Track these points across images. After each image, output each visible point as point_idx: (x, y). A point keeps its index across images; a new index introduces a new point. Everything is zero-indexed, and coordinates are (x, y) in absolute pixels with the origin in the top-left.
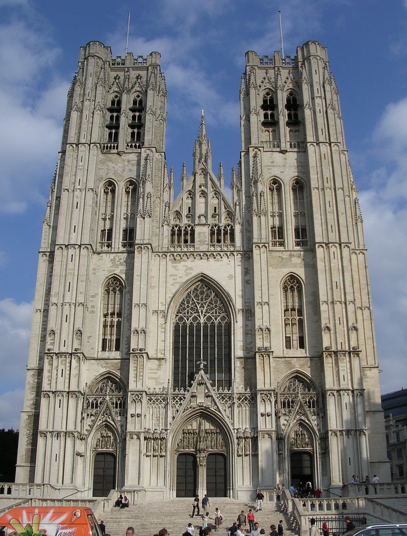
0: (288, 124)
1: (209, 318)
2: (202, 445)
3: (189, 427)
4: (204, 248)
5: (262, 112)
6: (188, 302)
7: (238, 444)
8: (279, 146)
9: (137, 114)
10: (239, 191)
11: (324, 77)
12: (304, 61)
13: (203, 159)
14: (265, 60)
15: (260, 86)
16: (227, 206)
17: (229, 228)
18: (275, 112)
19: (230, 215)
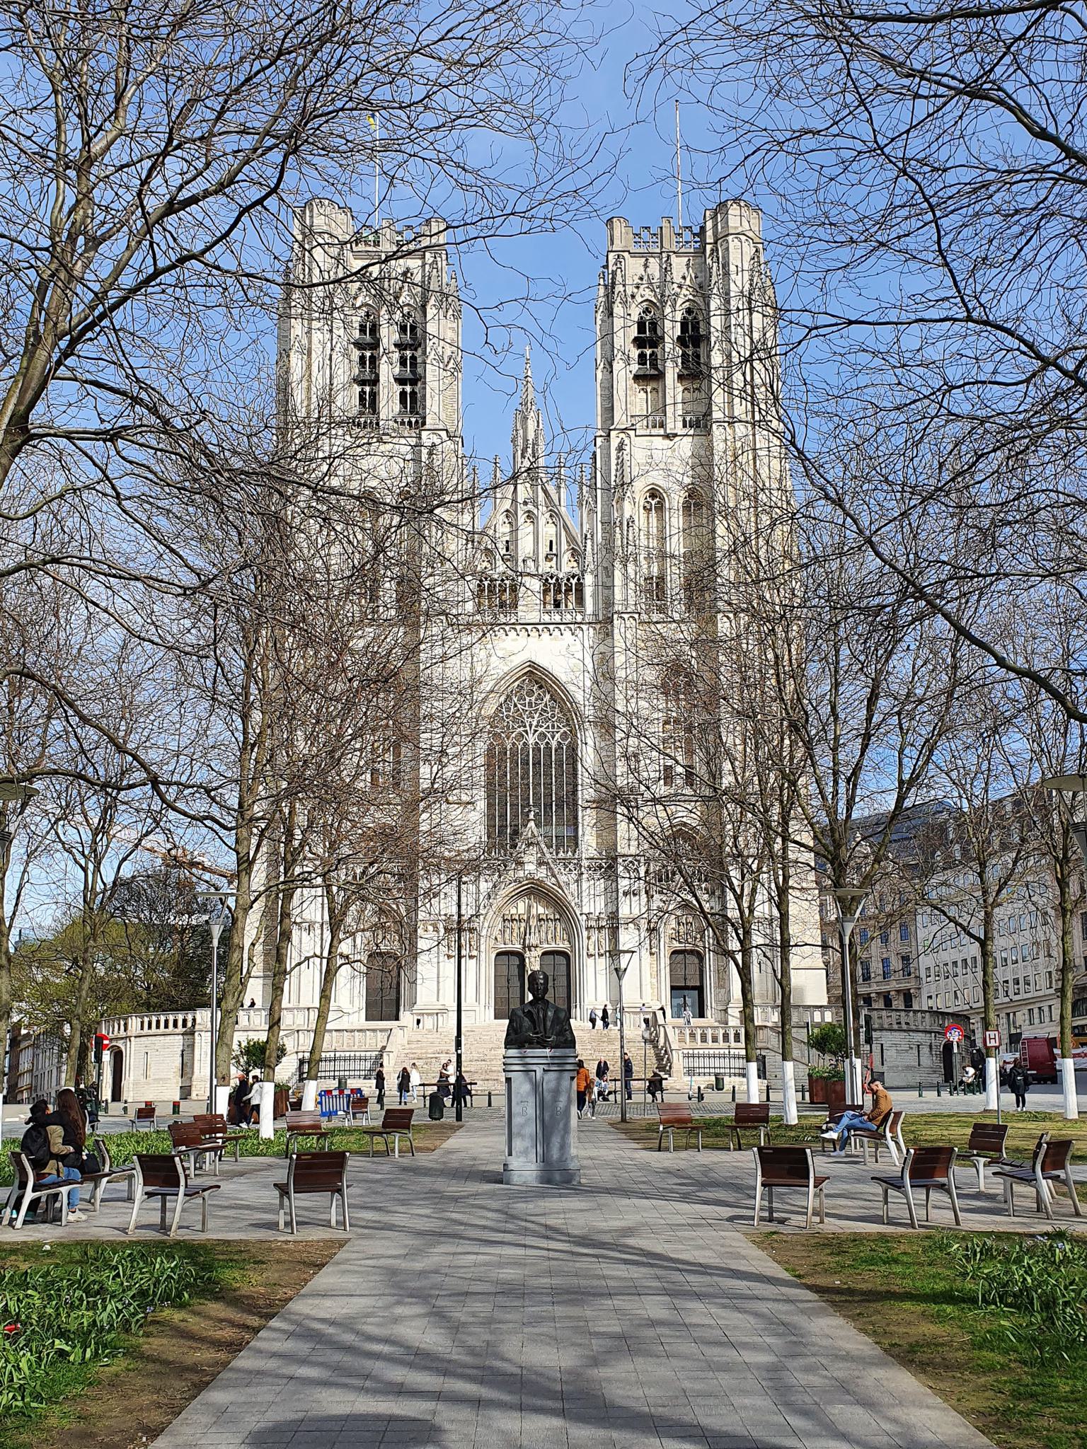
0: (681, 377)
1: (543, 736)
2: (533, 940)
3: (513, 911)
4: (533, 617)
5: (635, 353)
6: (508, 710)
7: (589, 938)
8: (662, 425)
9: (408, 353)
10: (592, 511)
11: (751, 280)
12: (716, 243)
13: (530, 451)
14: (645, 235)
15: (633, 297)
16: (571, 538)
17: (574, 581)
18: (658, 351)
19: (577, 554)
